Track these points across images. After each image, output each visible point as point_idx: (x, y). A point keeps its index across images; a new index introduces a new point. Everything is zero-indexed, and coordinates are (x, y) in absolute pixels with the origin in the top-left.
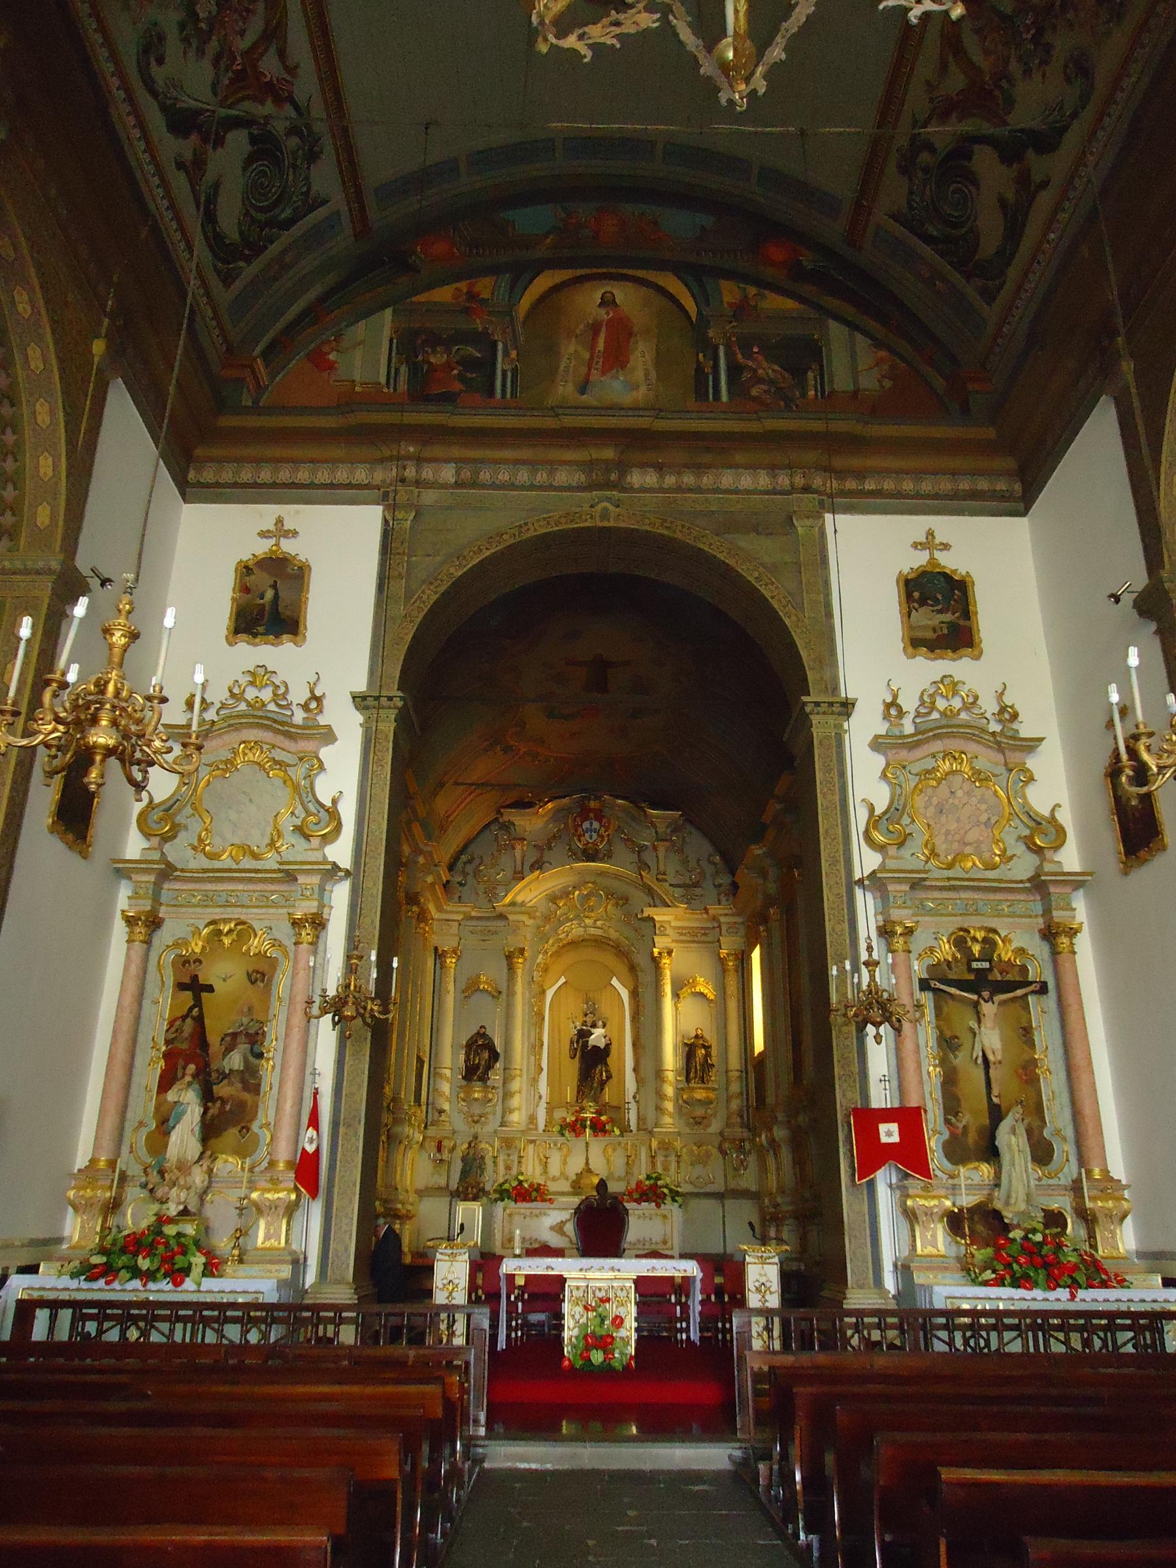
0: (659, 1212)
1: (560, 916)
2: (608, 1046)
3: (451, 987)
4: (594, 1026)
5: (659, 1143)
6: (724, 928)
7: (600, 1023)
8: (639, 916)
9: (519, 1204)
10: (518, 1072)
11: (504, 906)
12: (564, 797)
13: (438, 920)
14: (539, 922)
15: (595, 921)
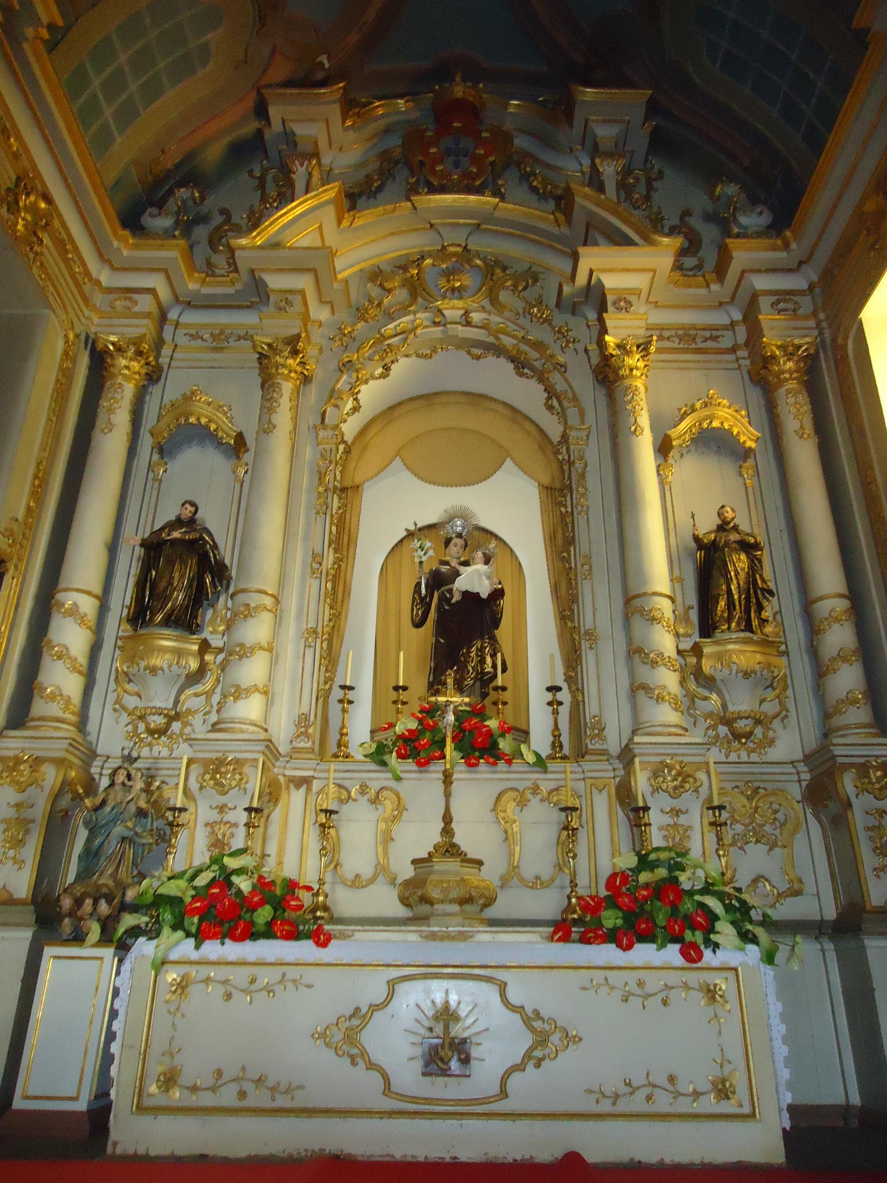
0: (694, 978)
1: (391, 307)
2: (498, 594)
3: (122, 419)
4: (466, 564)
5: (656, 774)
6: (765, 302)
7: (479, 555)
8: (566, 289)
9: (212, 949)
10: (268, 601)
11: (254, 248)
12: (401, 97)
13: (110, 290)
14: (343, 315)
15: (467, 313)
